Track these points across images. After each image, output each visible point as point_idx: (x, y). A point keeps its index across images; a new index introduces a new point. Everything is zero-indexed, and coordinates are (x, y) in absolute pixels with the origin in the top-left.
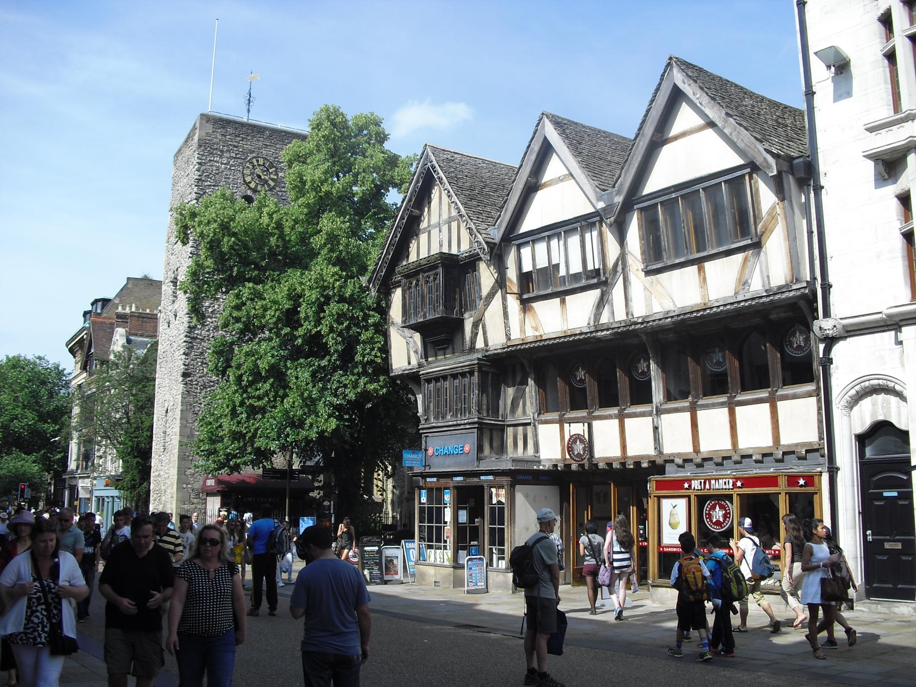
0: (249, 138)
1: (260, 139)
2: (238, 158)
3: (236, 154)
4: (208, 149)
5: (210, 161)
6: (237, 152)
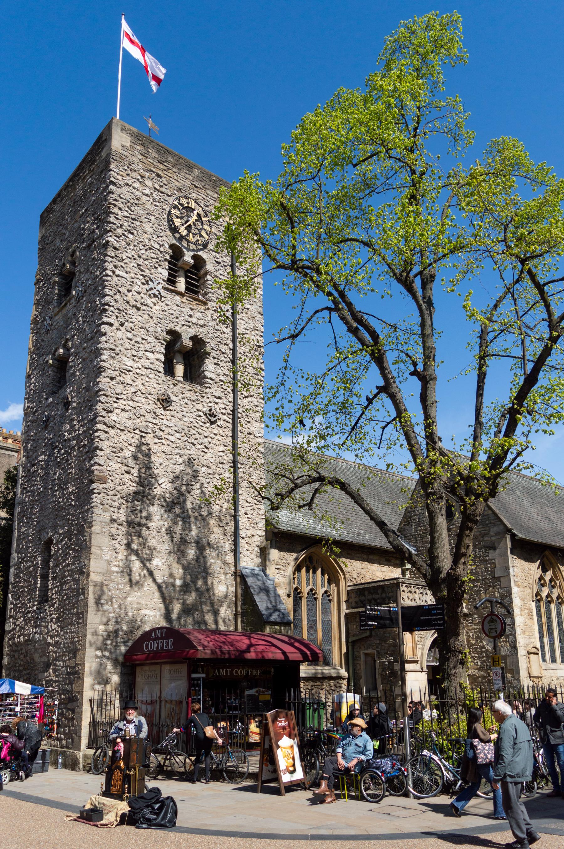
0: (174, 170)
1: (187, 176)
2: (162, 192)
3: (161, 186)
4: (126, 168)
5: (127, 184)
6: (162, 184)
